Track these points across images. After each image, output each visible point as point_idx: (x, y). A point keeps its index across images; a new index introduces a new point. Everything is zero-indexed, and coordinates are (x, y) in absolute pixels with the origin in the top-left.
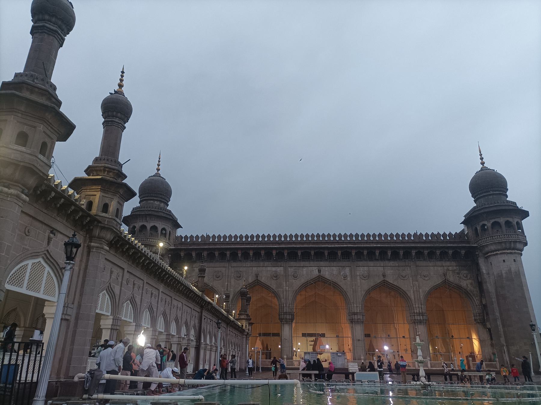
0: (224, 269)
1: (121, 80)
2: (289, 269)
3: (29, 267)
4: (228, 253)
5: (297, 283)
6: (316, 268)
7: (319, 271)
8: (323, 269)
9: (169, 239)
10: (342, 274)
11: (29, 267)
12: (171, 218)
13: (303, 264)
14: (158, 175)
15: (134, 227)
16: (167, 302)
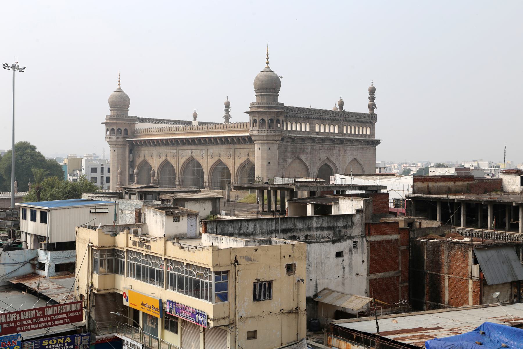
5: (182, 161)
7: (192, 153)
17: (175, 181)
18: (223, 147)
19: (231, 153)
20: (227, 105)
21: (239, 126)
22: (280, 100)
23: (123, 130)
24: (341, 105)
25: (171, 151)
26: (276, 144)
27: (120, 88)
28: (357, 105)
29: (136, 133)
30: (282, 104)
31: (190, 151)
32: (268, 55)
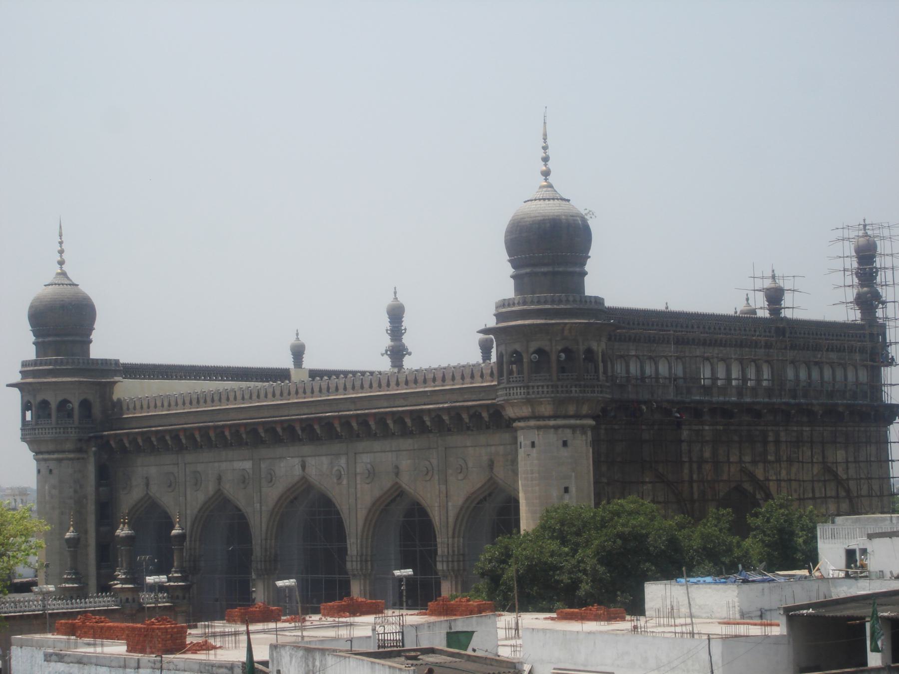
5: (273, 493)
6: (297, 461)
7: (304, 467)
10: (336, 468)
17: (344, 562)
18: (407, 444)
19: (434, 462)
20: (396, 315)
21: (458, 377)
22: (592, 287)
23: (76, 405)
24: (775, 296)
25: (239, 465)
26: (583, 428)
27: (63, 274)
28: (822, 298)
29: (113, 412)
30: (599, 301)
31: (297, 461)
32: (545, 148)
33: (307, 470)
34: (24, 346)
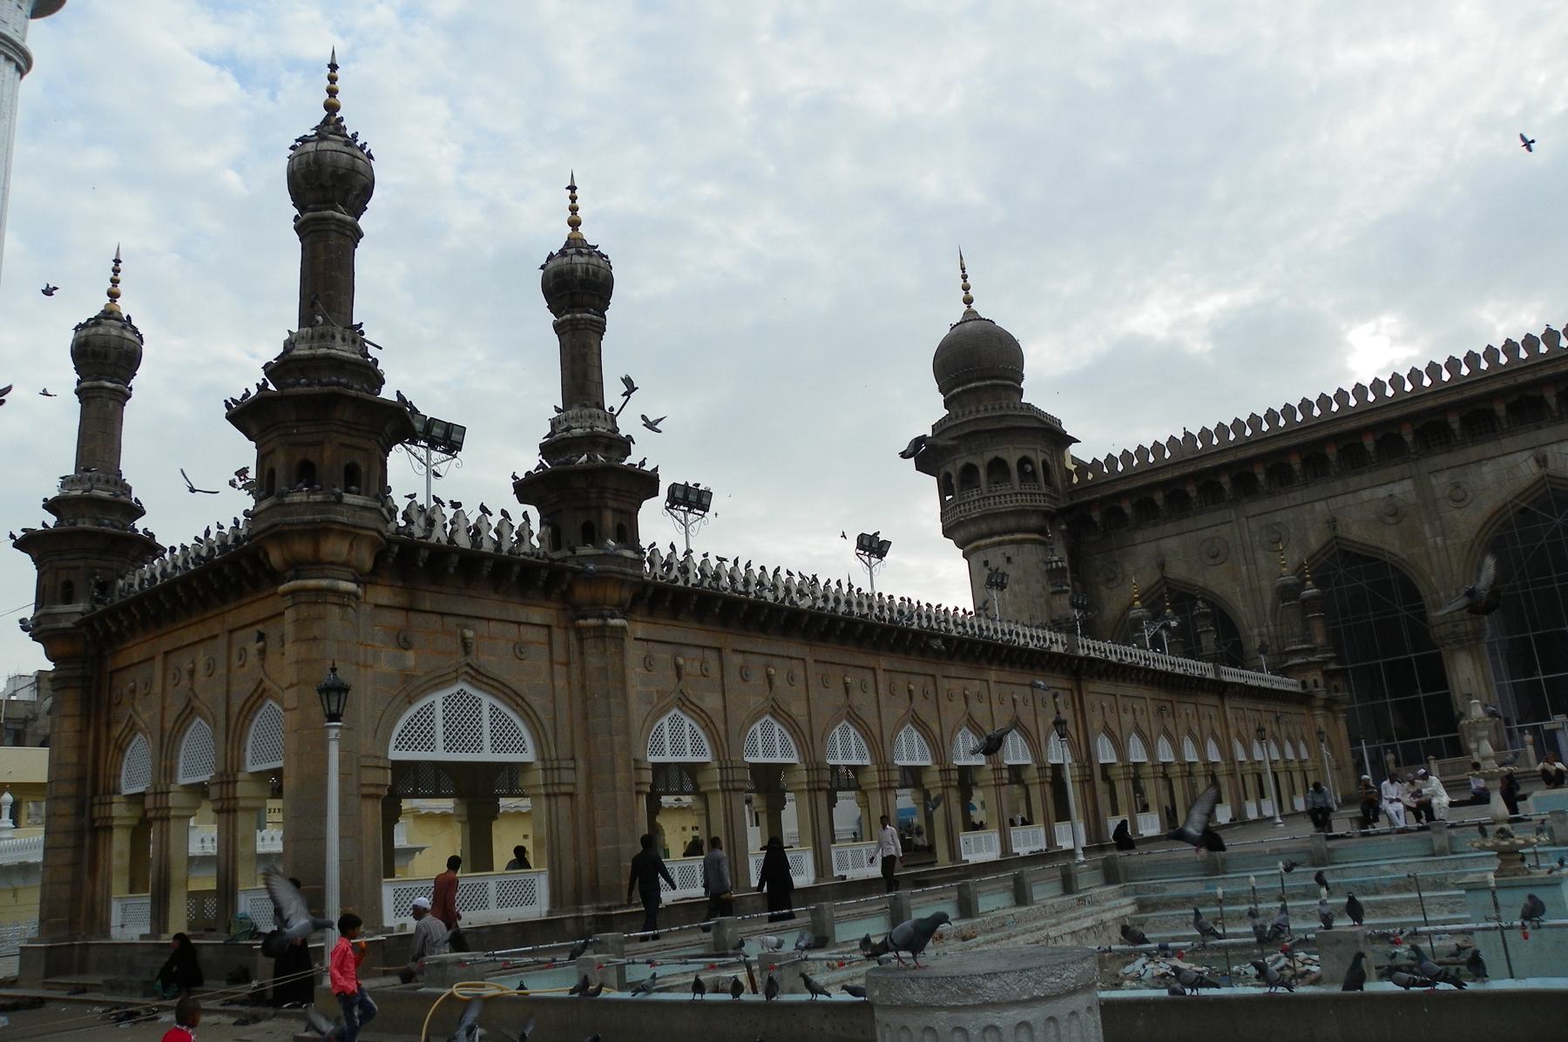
0: (1225, 529)
1: (574, 210)
2: (1434, 481)
3: (439, 707)
4: (1225, 480)
5: (1469, 521)
6: (1527, 454)
7: (1542, 461)
8: (1551, 451)
9: (1048, 482)
11: (439, 707)
12: (1037, 425)
13: (1474, 452)
14: (970, 316)
15: (948, 476)
16: (917, 695)
33: (1551, 465)
34: (926, 410)
